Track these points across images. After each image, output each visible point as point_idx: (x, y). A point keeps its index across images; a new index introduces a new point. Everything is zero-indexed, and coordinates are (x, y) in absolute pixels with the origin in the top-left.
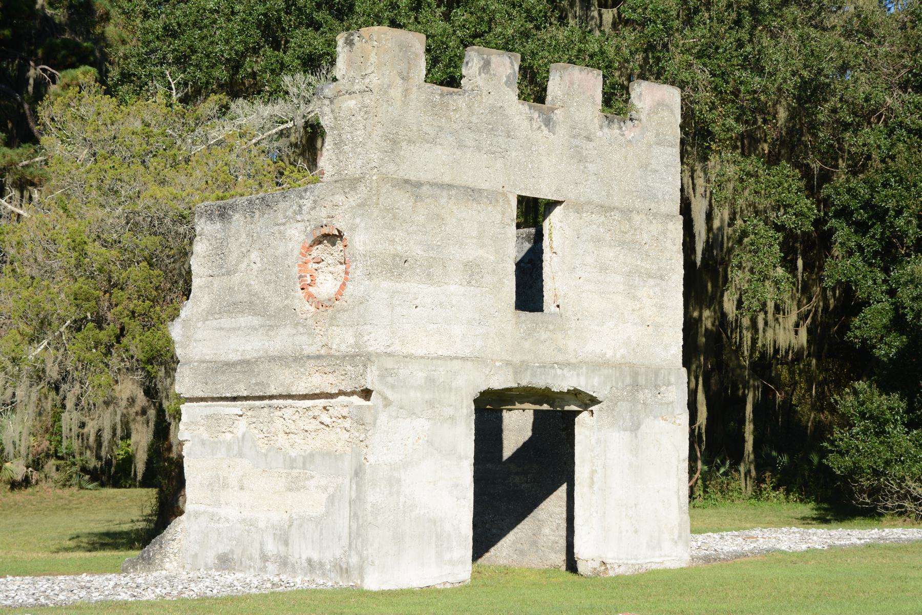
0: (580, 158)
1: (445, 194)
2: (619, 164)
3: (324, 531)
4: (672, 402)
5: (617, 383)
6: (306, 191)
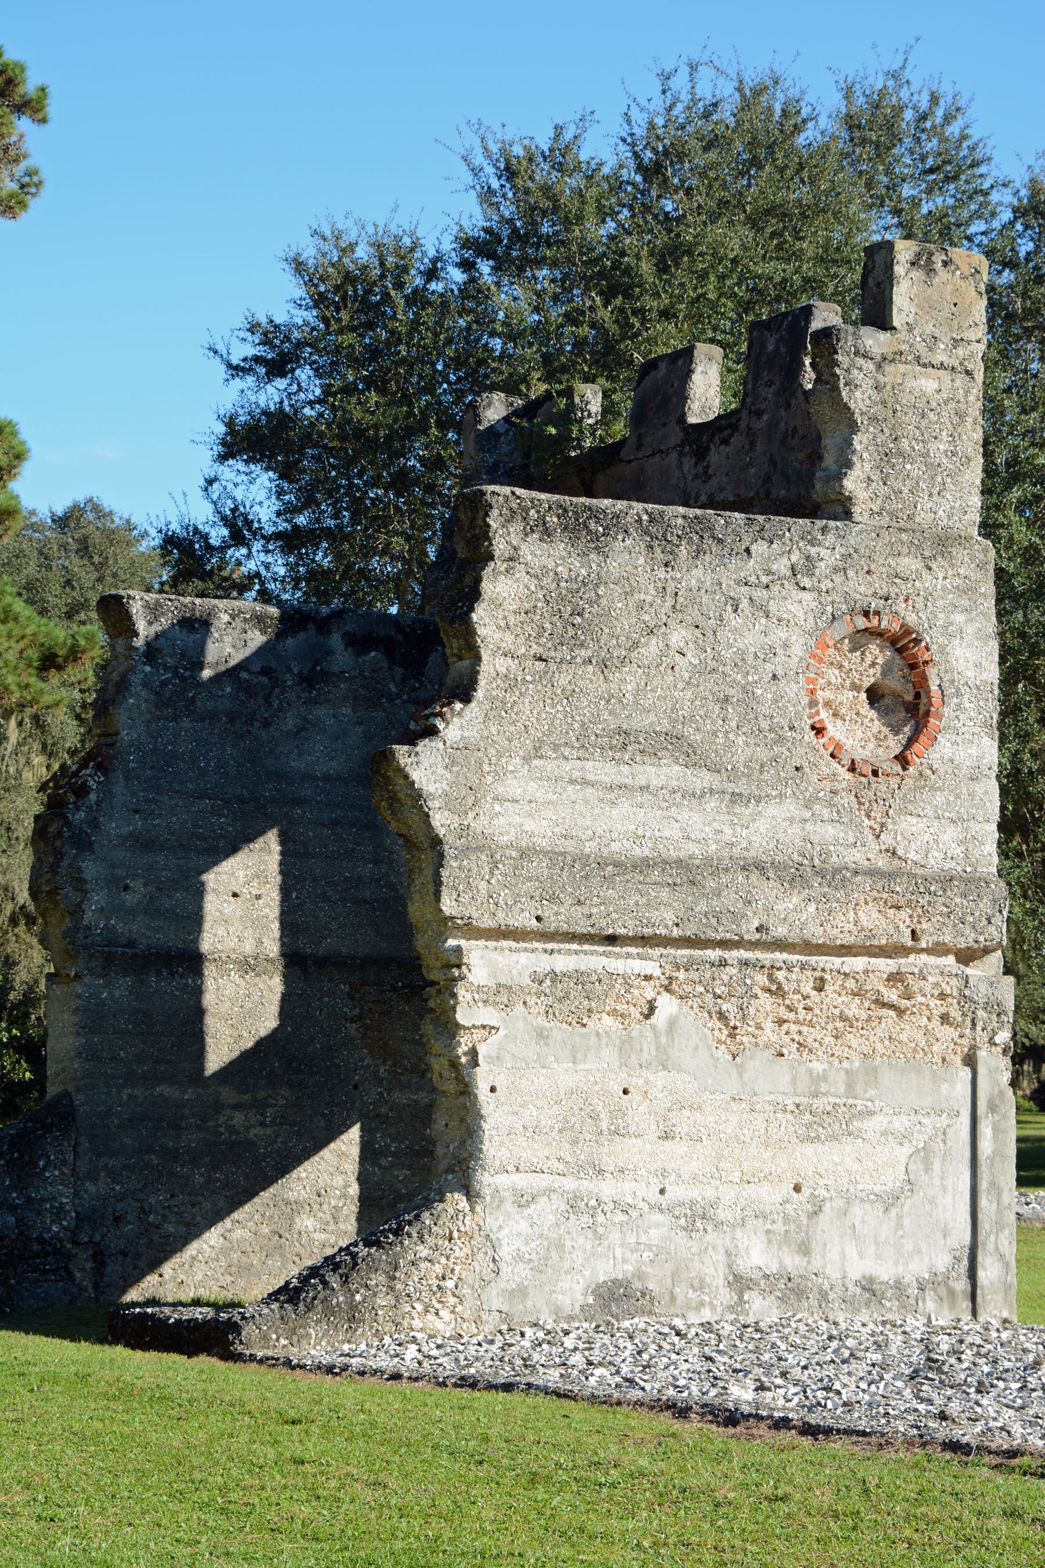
3: (906, 1221)
6: (824, 530)
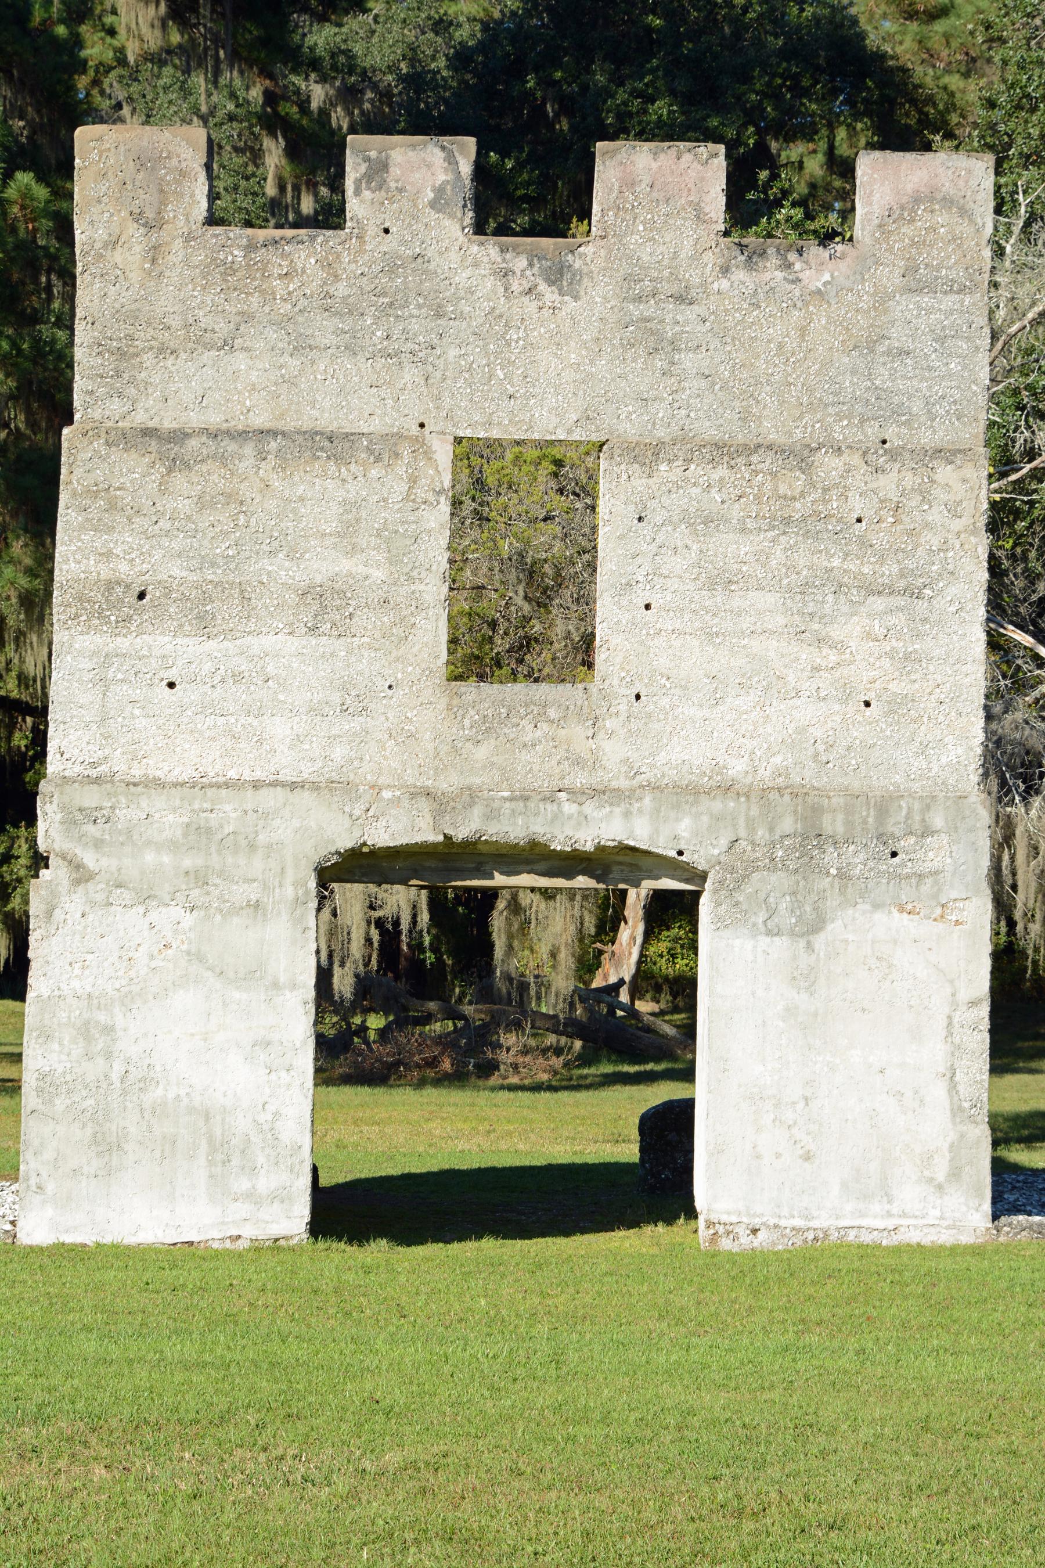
0: (660, 344)
1: (249, 450)
2: (780, 346)
4: (937, 873)
5: (751, 829)
